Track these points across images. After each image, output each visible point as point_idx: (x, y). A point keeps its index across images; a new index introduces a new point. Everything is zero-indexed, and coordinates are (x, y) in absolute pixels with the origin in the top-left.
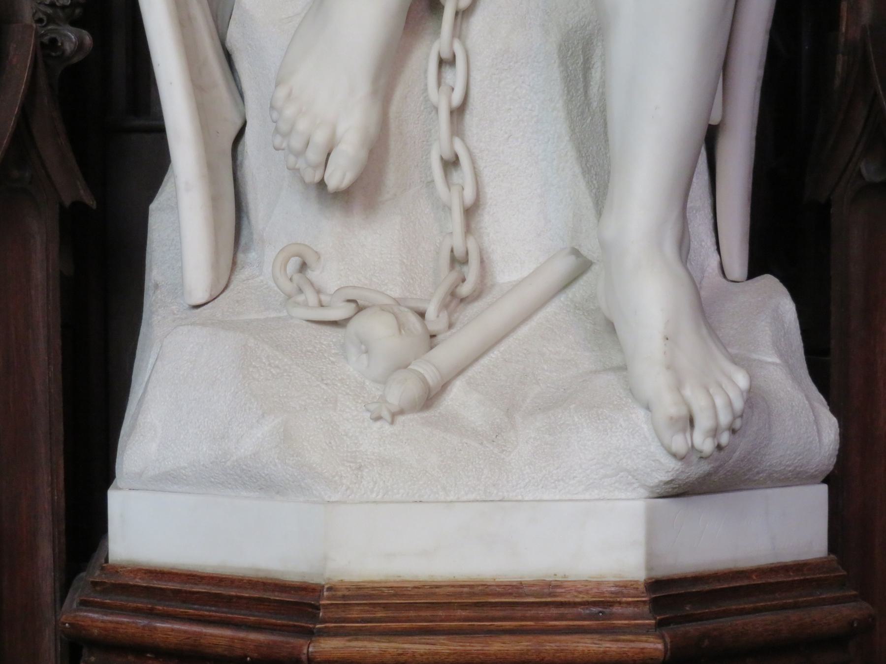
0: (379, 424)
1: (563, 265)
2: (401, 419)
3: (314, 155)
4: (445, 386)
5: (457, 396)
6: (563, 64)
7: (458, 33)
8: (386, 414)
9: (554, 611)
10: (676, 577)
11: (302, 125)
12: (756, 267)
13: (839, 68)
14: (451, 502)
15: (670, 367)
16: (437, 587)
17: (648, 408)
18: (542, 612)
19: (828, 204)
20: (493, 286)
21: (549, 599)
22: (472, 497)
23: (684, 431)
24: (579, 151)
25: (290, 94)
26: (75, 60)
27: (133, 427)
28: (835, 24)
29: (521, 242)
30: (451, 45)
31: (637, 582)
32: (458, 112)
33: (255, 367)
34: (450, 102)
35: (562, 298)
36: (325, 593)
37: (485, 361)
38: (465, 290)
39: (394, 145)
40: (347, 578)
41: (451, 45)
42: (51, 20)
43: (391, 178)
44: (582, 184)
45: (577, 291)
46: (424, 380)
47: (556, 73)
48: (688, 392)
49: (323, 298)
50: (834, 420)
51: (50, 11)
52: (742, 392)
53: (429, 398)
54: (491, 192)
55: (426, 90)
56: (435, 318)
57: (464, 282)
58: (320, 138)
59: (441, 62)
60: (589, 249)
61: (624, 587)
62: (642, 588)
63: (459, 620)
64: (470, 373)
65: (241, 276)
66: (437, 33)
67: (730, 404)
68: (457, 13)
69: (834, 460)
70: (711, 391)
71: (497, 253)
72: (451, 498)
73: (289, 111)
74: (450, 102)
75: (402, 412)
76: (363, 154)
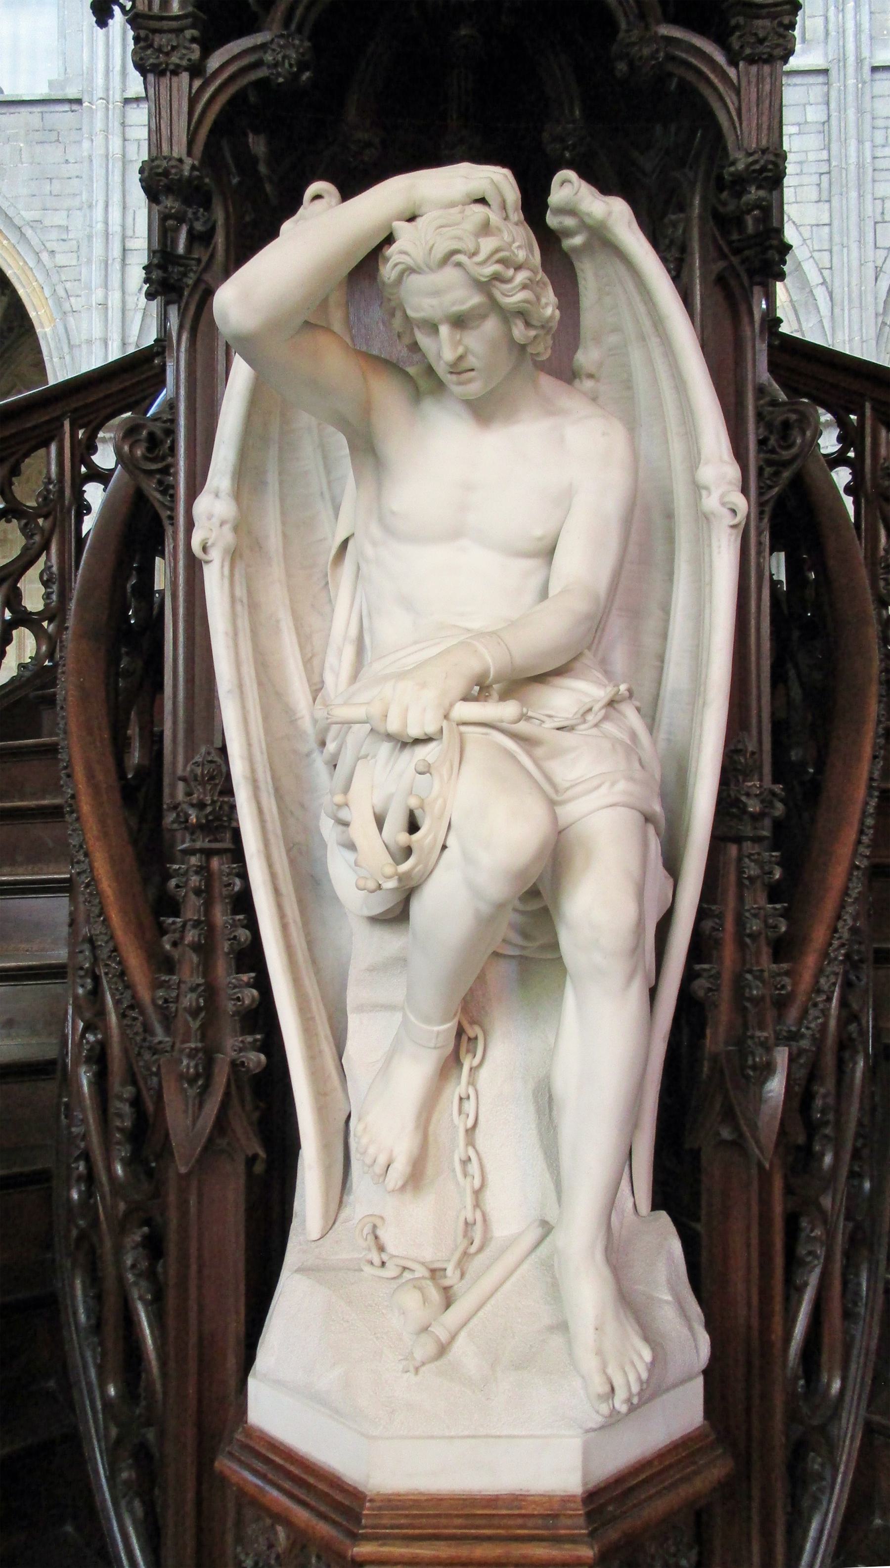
0: (408, 1374)
1: (534, 1234)
2: (423, 1369)
3: (378, 1169)
4: (453, 1337)
5: (462, 1347)
6: (536, 1102)
7: (472, 1082)
8: (412, 1369)
9: (520, 1521)
10: (602, 1485)
11: (372, 1150)
12: (656, 1206)
13: (705, 1069)
14: (452, 1437)
15: (599, 1353)
16: (441, 1500)
17: (583, 1377)
18: (511, 1522)
19: (700, 1149)
20: (491, 1238)
21: (517, 1512)
22: (466, 1433)
23: (607, 1400)
24: (546, 1154)
25: (365, 1129)
26: (257, 1071)
27: (262, 1343)
28: (703, 1036)
29: (510, 1211)
30: (467, 1090)
31: (574, 1496)
32: (471, 1132)
33: (333, 1321)
34: (466, 1124)
35: (533, 1256)
36: (368, 1504)
37: (480, 1314)
38: (473, 1249)
39: (432, 1151)
40: (383, 1490)
41: (467, 1090)
42: (241, 1050)
43: (430, 1170)
44: (548, 1176)
45: (543, 1250)
46: (439, 1340)
47: (532, 1108)
48: (610, 1371)
49: (385, 1257)
50: (707, 1337)
51: (241, 1045)
52: (647, 1364)
53: (443, 1349)
54: (491, 1178)
55: (452, 1114)
56: (451, 1277)
57: (474, 1237)
58: (382, 1160)
59: (461, 1099)
60: (551, 1218)
61: (566, 1500)
62: (579, 1500)
63: (455, 1527)
64: (471, 1325)
65: (345, 1213)
66: (459, 1077)
67: (639, 1378)
68: (471, 1069)
69: (707, 1362)
70: (626, 1369)
71: (495, 1216)
72: (453, 1434)
73: (364, 1141)
74: (466, 1124)
75: (423, 1364)
76: (408, 1169)
